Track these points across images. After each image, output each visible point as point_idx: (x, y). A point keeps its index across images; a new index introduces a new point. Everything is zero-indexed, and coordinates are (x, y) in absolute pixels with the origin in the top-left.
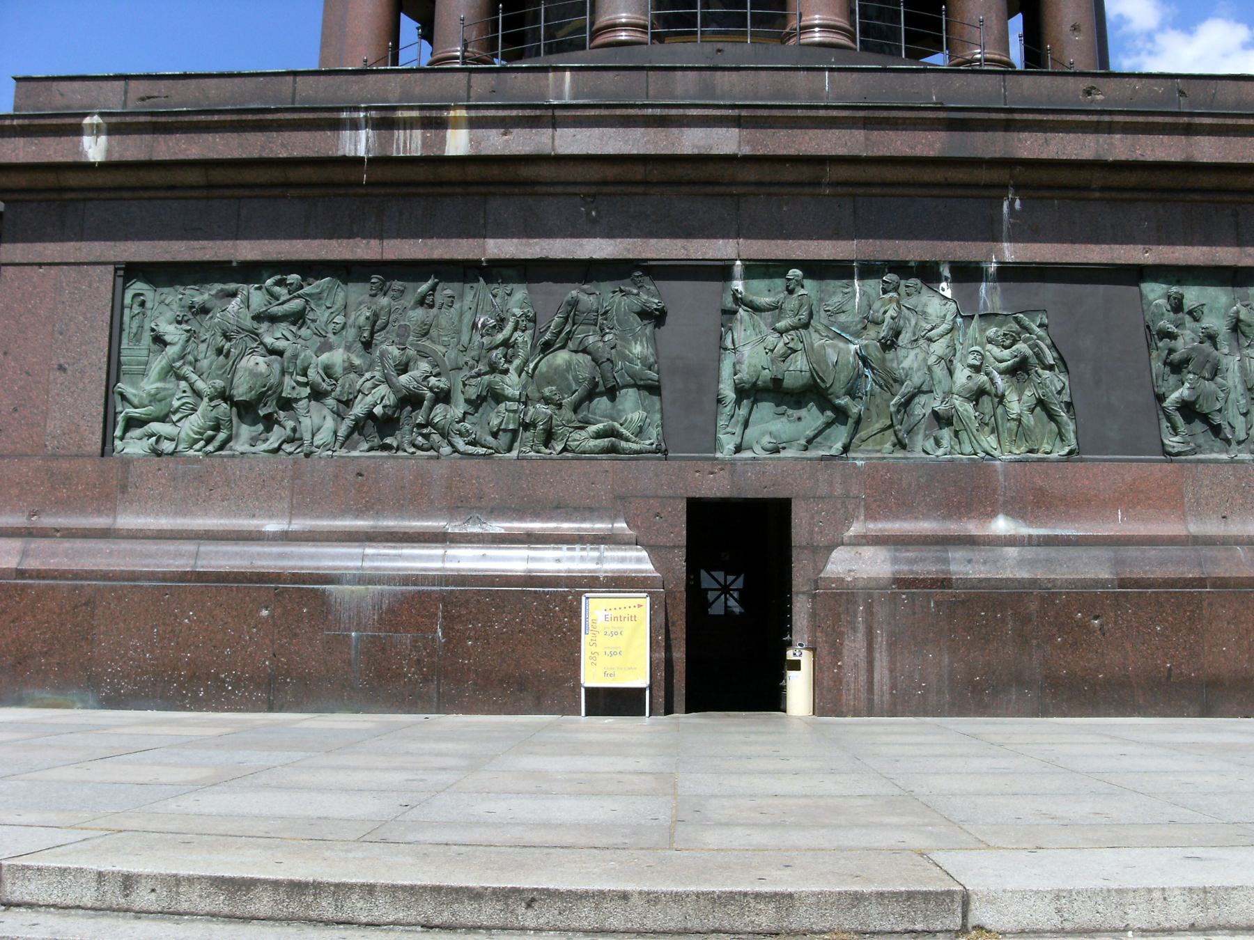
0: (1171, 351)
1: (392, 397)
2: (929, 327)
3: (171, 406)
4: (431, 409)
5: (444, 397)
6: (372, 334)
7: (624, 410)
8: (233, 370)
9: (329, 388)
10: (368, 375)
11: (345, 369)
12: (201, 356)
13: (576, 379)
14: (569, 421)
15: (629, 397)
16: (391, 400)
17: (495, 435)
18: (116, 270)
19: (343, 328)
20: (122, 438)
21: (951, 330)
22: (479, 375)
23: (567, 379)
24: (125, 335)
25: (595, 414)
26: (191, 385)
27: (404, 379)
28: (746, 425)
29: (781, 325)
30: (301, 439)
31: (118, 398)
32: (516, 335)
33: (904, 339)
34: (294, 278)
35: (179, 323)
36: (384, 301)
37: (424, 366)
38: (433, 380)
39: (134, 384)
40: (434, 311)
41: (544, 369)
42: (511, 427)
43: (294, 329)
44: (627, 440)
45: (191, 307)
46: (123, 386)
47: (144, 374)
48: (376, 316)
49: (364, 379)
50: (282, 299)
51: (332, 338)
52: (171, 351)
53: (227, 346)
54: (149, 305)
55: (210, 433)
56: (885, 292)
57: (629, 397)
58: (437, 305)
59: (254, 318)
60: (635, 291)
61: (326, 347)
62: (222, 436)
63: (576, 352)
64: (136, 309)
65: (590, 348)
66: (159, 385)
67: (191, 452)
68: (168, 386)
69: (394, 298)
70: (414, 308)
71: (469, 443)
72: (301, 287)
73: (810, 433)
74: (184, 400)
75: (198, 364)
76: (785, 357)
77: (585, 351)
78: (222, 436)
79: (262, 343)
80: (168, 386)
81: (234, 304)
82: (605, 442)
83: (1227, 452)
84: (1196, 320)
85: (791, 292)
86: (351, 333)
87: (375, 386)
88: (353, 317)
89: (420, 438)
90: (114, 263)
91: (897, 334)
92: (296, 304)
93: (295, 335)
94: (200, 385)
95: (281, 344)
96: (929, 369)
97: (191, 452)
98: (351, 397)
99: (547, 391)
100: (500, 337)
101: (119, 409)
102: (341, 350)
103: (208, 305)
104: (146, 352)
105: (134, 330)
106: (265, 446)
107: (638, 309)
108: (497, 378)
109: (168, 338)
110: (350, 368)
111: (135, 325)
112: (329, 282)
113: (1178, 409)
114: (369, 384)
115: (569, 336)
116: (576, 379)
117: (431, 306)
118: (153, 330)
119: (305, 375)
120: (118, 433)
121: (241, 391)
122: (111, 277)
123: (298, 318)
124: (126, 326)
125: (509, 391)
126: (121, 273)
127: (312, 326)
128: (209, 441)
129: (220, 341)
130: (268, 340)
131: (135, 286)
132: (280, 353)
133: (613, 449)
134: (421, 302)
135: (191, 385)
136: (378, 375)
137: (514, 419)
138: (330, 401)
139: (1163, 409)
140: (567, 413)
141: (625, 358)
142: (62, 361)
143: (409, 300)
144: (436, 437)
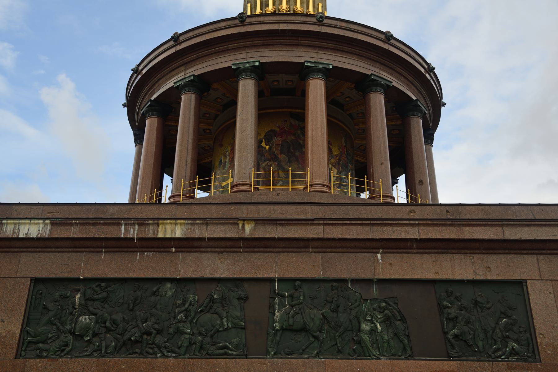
0: (449, 314)
1: (139, 333)
2: (350, 304)
4: (155, 337)
5: (159, 332)
6: (133, 307)
17: (179, 348)
18: (31, 280)
20: (25, 350)
21: (359, 306)
26: (58, 328)
28: (278, 343)
29: (293, 303)
30: (101, 350)
31: (25, 333)
33: (341, 309)
34: (103, 284)
36: (139, 293)
40: (158, 297)
43: (102, 304)
44: (232, 350)
48: (136, 299)
52: (51, 314)
54: (43, 295)
56: (333, 290)
60: (237, 290)
71: (168, 352)
72: (107, 288)
73: (304, 347)
76: (293, 316)
77: (216, 313)
79: (89, 310)
82: (222, 351)
83: (475, 356)
84: (459, 301)
85: (296, 290)
90: (31, 278)
91: (339, 307)
92: (104, 295)
93: (103, 307)
96: (351, 321)
100: (183, 308)
101: (25, 338)
109: (50, 308)
113: (453, 338)
114: (130, 327)
115: (211, 308)
118: (44, 305)
122: (29, 283)
123: (104, 300)
126: (33, 281)
128: (63, 350)
130: (91, 309)
134: (154, 293)
135: (58, 328)
136: (134, 323)
139: (447, 338)
140: (208, 339)
142: (3, 318)
144: (156, 349)
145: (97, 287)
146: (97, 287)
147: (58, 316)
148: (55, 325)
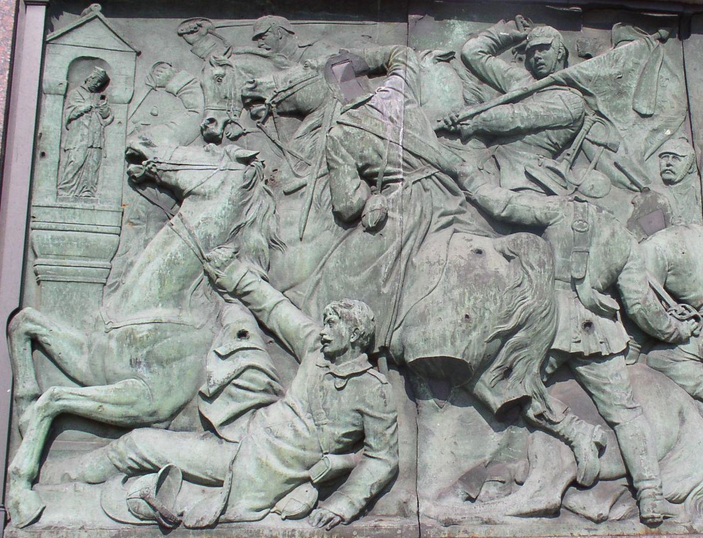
3: (202, 375)
8: (403, 267)
12: (288, 234)
24: (46, 168)
35: (214, 139)
39: (69, 312)
45: (251, 101)
46: (39, 319)
47: (106, 283)
50: (515, 90)
51: (667, 196)
53: (377, 202)
54: (117, 90)
55: (337, 462)
59: (440, 132)
61: (649, 219)
62: (371, 472)
64: (83, 100)
66: (163, 313)
67: (273, 522)
68: (188, 317)
74: (242, 361)
75: (281, 258)
78: (371, 472)
80: (188, 317)
81: (387, 95)
92: (560, 103)
94: (288, 318)
95: (531, 205)
97: (273, 522)
103: (304, 96)
104: (109, 220)
105: (77, 157)
106: (523, 498)
109: (185, 179)
111: (79, 139)
112: (639, 53)
118: (135, 157)
120: (24, 458)
121: (436, 334)
123: (565, 140)
124: (50, 143)
129: (354, 190)
131: (78, 37)
132: (538, 228)
145: (498, 48)
146: (498, 48)
147: (255, 238)
148: (240, 295)
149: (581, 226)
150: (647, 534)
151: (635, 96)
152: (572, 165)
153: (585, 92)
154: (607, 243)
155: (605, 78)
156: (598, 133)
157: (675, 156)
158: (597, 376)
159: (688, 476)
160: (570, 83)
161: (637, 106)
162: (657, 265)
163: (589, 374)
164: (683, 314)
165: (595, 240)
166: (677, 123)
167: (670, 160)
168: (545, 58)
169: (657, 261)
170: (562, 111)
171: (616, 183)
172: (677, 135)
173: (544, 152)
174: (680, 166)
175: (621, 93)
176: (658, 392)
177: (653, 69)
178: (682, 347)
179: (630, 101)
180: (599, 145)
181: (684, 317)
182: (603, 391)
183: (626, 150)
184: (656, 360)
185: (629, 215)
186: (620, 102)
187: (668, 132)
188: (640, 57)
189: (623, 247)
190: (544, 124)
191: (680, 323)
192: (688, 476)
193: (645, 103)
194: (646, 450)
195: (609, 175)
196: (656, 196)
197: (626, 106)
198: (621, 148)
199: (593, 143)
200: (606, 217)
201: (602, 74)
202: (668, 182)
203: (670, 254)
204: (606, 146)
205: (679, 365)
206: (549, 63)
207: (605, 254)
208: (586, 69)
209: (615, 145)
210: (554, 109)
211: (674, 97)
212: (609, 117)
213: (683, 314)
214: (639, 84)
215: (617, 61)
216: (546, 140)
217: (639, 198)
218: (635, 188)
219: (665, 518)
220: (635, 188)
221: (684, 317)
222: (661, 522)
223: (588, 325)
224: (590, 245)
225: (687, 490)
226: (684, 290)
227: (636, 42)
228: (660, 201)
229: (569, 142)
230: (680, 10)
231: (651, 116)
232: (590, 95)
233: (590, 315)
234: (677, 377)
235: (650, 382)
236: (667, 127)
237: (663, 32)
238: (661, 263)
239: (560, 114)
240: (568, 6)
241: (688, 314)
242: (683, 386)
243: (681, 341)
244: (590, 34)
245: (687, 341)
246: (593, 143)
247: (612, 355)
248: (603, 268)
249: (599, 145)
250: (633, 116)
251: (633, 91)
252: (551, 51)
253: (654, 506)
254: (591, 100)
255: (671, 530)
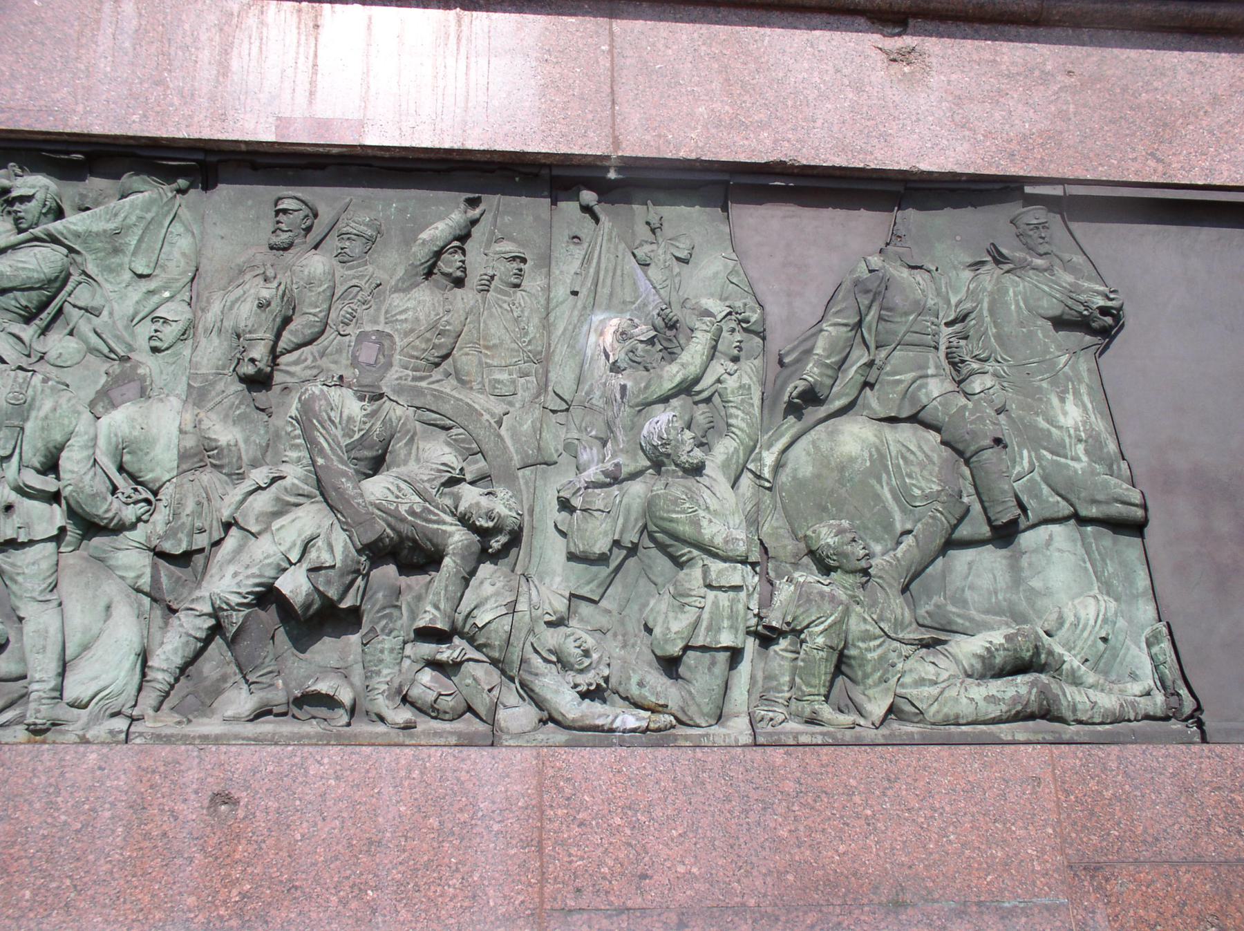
5: (497, 543)
6: (274, 355)
7: (1047, 592)
9: (129, 514)
10: (259, 475)
11: (183, 456)
13: (904, 497)
14: (899, 624)
15: (1055, 555)
16: (337, 548)
17: (670, 666)
19: (183, 336)
22: (614, 479)
23: (878, 497)
25: (964, 603)
27: (377, 488)
32: (718, 368)
37: (439, 453)
38: (470, 496)
40: (465, 298)
41: (807, 470)
42: (726, 639)
43: (28, 332)
44: (1076, 681)
49: (247, 486)
51: (149, 365)
57: (1055, 555)
58: (473, 280)
63: (892, 420)
65: (936, 411)
69: (343, 258)
70: (405, 287)
72: (59, 214)
86: (210, 352)
87: (283, 508)
88: (216, 308)
89: (427, 676)
98: (201, 541)
99: (826, 536)
100: (672, 374)
102: (175, 402)
107: (1056, 311)
108: (678, 487)
110: (202, 456)
112: (147, 207)
114: (262, 502)
116: (904, 497)
117: (459, 282)
119: (51, 466)
125: (713, 531)
127: (85, 328)
133: (1048, 713)
136: (295, 474)
137: (732, 616)
138: (130, 557)
141: (1037, 439)
143: (391, 263)
149: (14, 398)
150: (29, 742)
151: (134, 254)
152: (44, 331)
153: (71, 250)
154: (46, 417)
155: (97, 234)
156: (83, 296)
157: (166, 321)
158: (13, 565)
159: (96, 678)
160: (54, 239)
161: (133, 265)
162: (109, 443)
163: (5, 563)
164: (129, 497)
165: (33, 414)
166: (180, 284)
167: (158, 325)
168: (25, 211)
169: (109, 438)
170: (33, 270)
171: (93, 350)
172: (179, 297)
173: (10, 316)
174: (170, 333)
175: (116, 251)
176: (87, 584)
177: (161, 224)
178: (127, 533)
179: (126, 260)
180: (80, 308)
181: (130, 500)
182: (16, 582)
183: (111, 314)
184: (96, 547)
185: (99, 387)
186: (115, 260)
187: (167, 294)
188: (148, 210)
189: (66, 421)
190: (10, 285)
191: (124, 507)
192: (96, 678)
193: (144, 262)
194: (44, 648)
195: (85, 341)
196: (138, 364)
197: (121, 265)
198: (105, 313)
199: (75, 306)
200: (52, 389)
201: (95, 228)
202: (155, 350)
203: (125, 430)
204: (87, 310)
205: (120, 554)
206: (29, 217)
207: (43, 429)
208: (75, 224)
209: (96, 309)
210: (24, 269)
211: (184, 254)
212: (99, 279)
213: (129, 497)
214: (140, 241)
215: (116, 215)
216: (13, 302)
217: (116, 367)
218: (113, 356)
219: (54, 725)
220: (113, 356)
221: (130, 500)
222: (48, 730)
223: (9, 508)
224: (26, 419)
225: (90, 693)
226: (140, 471)
227: (146, 194)
228: (141, 371)
229: (43, 306)
230: (200, 156)
231: (148, 276)
232: (78, 253)
233: (14, 497)
234: (118, 567)
235: (81, 572)
236: (165, 288)
237: (182, 183)
238: (114, 439)
239: (30, 274)
240: (68, 153)
241: (136, 497)
242: (122, 578)
243: (120, 528)
244: (96, 184)
245: (133, 526)
246: (75, 306)
247: (31, 543)
248: (40, 445)
249: (80, 308)
250: (127, 276)
251: (132, 247)
252: (33, 203)
253: (38, 711)
254: (78, 259)
255: (60, 738)
